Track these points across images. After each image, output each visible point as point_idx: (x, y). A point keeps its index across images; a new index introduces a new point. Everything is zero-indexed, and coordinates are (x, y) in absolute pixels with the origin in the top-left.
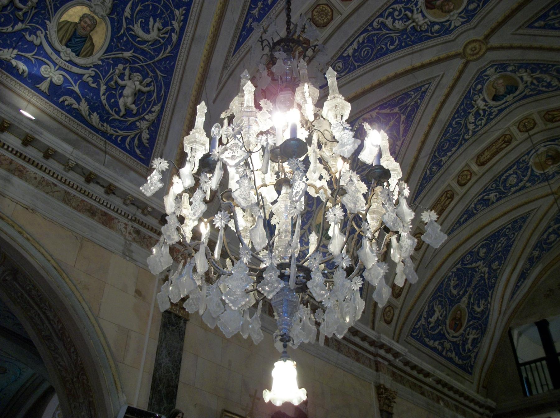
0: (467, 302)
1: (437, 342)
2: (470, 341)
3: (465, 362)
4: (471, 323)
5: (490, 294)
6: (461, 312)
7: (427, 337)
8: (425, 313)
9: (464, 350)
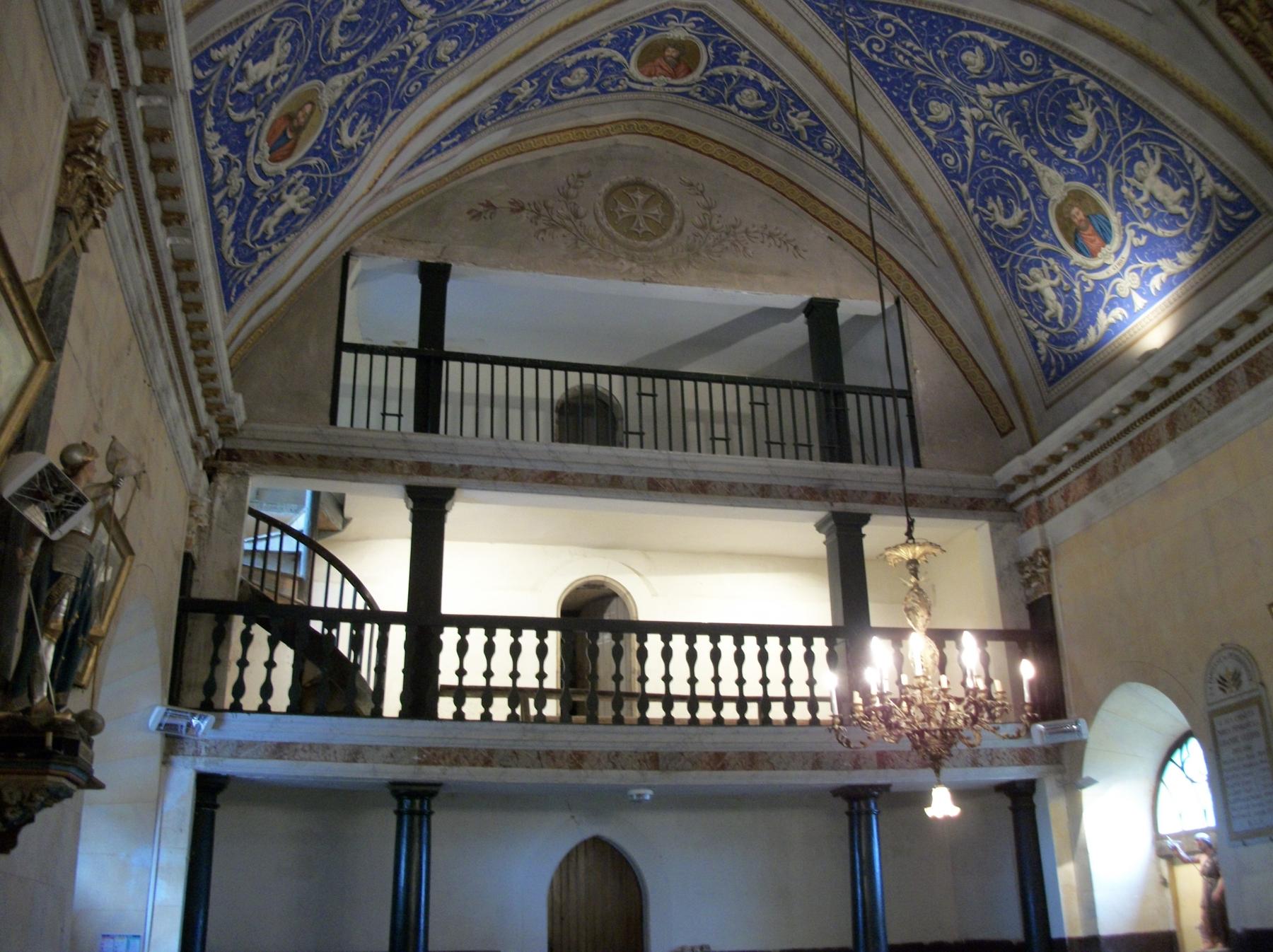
0: (338, 94)
1: (224, 150)
2: (281, 211)
3: (238, 265)
4: (313, 161)
5: (386, 119)
6: (312, 113)
7: (215, 111)
8: (250, 33)
9: (257, 224)
